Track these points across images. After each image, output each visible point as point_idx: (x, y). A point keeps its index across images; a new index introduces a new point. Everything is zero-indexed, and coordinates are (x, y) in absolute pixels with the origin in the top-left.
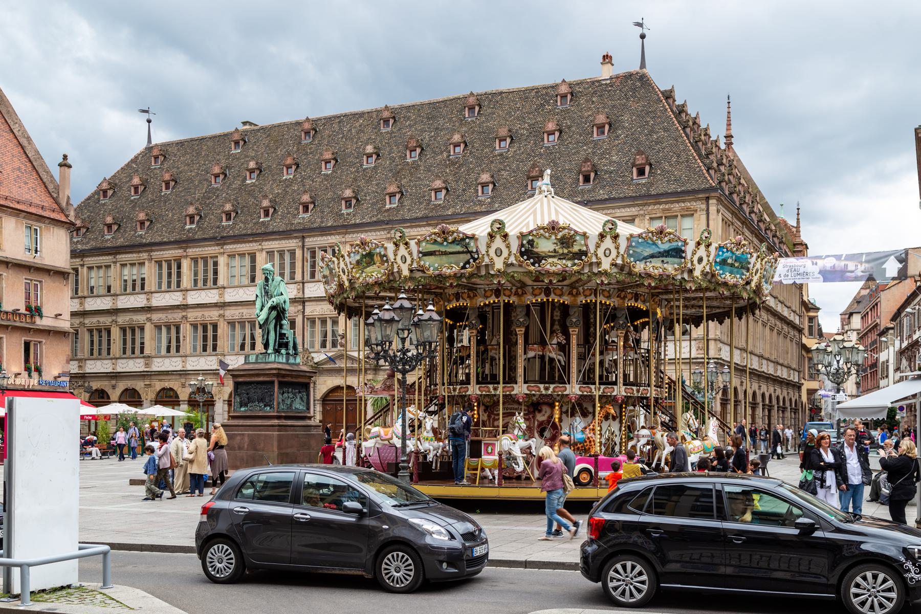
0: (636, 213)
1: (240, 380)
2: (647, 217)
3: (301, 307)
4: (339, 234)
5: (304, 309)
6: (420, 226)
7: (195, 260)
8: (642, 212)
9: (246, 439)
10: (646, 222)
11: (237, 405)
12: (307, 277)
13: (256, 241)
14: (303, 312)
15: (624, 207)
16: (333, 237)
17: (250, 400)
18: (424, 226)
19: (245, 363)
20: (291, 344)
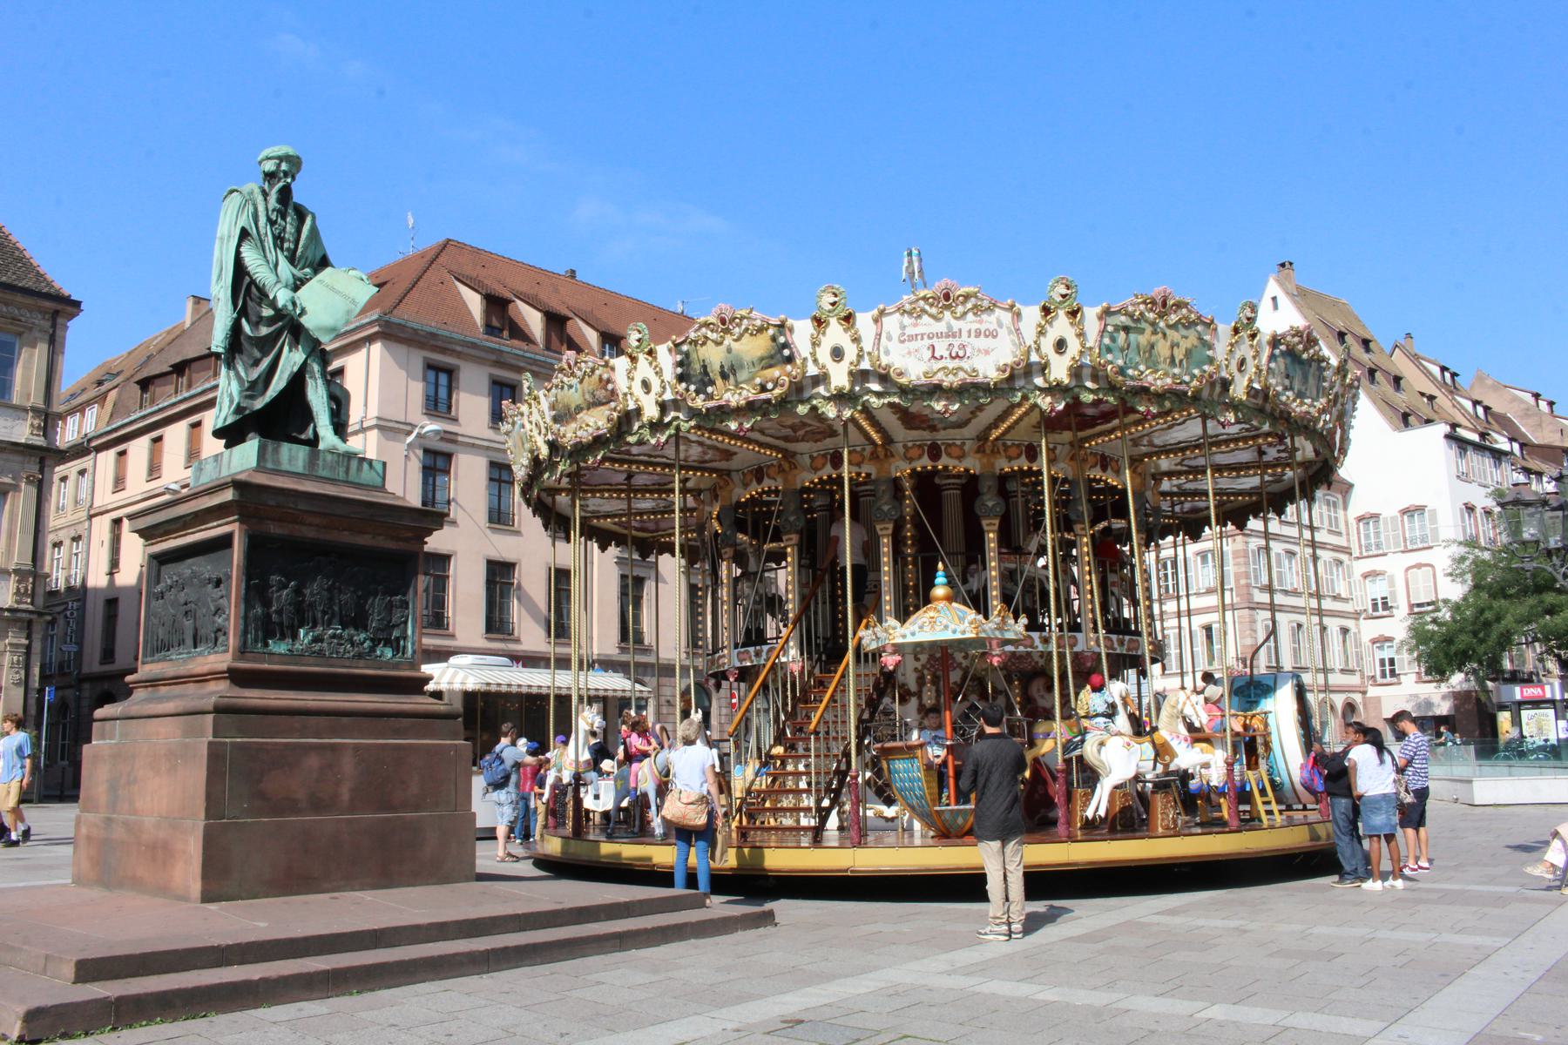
1: (274, 529)
9: (348, 765)
19: (261, 467)
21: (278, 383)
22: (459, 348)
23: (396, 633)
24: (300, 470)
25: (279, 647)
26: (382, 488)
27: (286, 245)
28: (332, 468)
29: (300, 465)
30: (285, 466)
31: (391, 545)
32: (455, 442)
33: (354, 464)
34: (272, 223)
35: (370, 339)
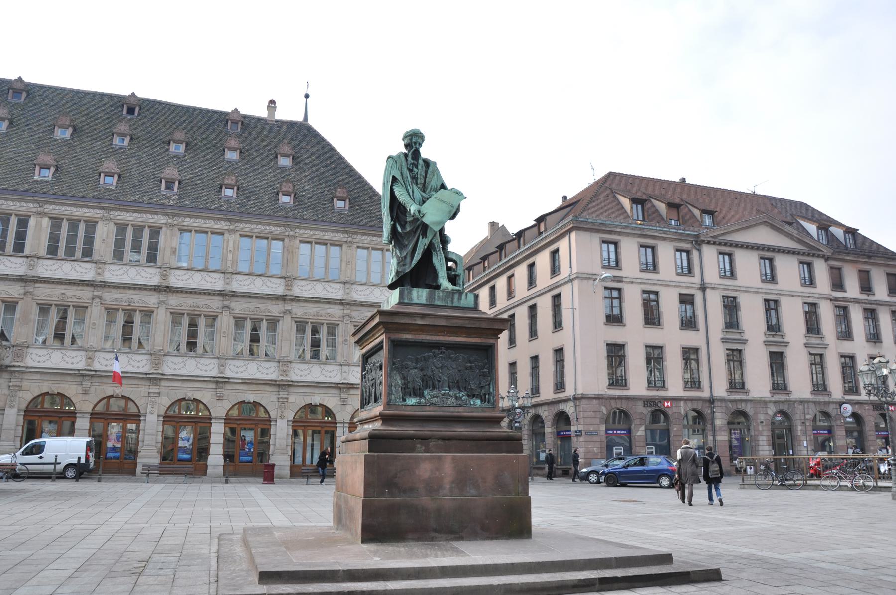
0: (345, 240)
6: (87, 207)
8: (350, 239)
11: (397, 393)
17: (430, 382)
18: (93, 208)
21: (417, 256)
22: (619, 230)
23: (483, 391)
24: (424, 302)
25: (411, 401)
26: (475, 309)
27: (419, 181)
29: (423, 300)
30: (415, 301)
32: (621, 281)
33: (456, 296)
34: (411, 171)
35: (569, 231)
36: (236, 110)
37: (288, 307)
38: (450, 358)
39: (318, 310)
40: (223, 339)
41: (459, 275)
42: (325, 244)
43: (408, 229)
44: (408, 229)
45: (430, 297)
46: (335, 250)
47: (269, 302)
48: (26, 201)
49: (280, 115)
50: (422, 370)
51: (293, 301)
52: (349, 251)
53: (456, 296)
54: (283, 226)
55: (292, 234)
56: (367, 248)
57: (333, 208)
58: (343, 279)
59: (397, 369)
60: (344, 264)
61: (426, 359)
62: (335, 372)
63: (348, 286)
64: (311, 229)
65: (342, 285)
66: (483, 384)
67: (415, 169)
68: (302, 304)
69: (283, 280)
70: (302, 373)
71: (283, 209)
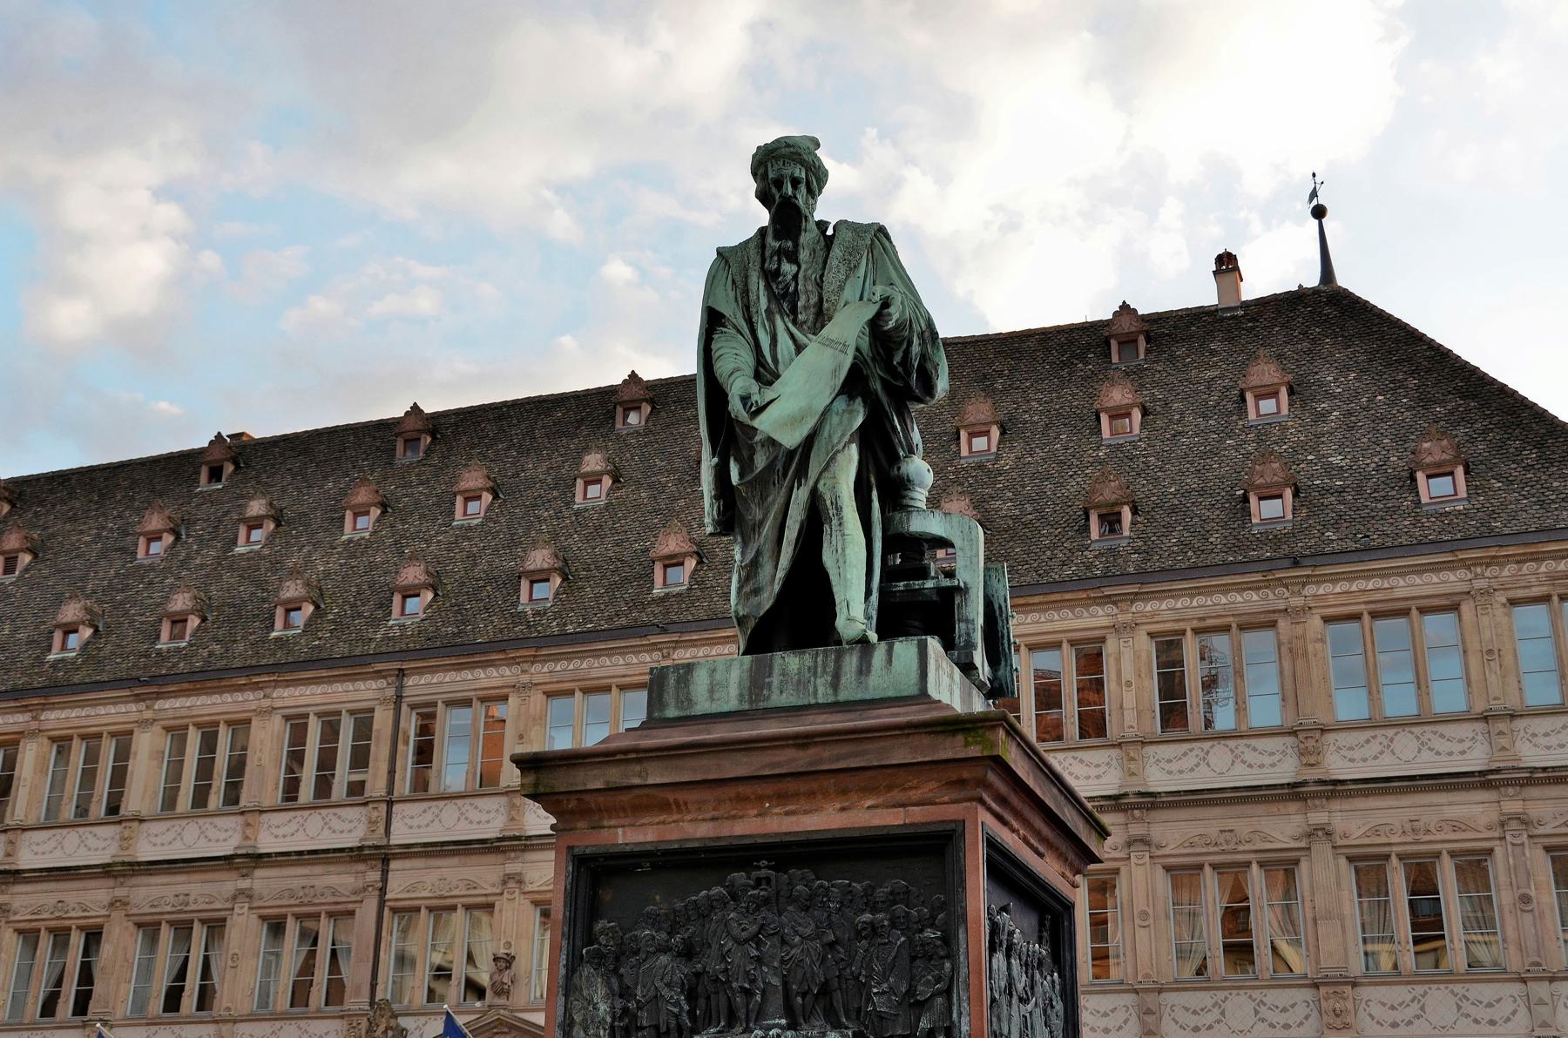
0: (1464, 587)
1: (628, 835)
2: (1501, 598)
3: (374, 876)
4: (512, 662)
5: (385, 880)
7: (62, 744)
8: (1480, 584)
10: (1499, 611)
12: (404, 786)
13: (256, 687)
14: (383, 891)
15: (1420, 570)
16: (493, 672)
20: (975, 611)
23: (924, 1024)
24: (732, 704)
26: (922, 696)
28: (801, 684)
30: (703, 705)
31: (891, 818)
33: (851, 662)
34: (771, 276)
36: (1125, 307)
37: (1318, 817)
38: (791, 899)
39: (1412, 813)
40: (1142, 934)
41: (963, 591)
42: (1405, 613)
43: (760, 461)
44: (760, 461)
45: (757, 683)
46: (1437, 627)
47: (1260, 809)
48: (636, 650)
49: (1256, 284)
50: (688, 953)
51: (1331, 796)
52: (1485, 620)
53: (851, 662)
54: (1267, 584)
55: (1297, 601)
56: (1545, 599)
57: (1418, 503)
58: (1480, 707)
59: (598, 959)
60: (1474, 663)
61: (703, 913)
62: (1506, 1007)
63: (1501, 726)
64: (1352, 577)
65: (1480, 726)
66: (923, 992)
67: (788, 268)
68: (1360, 803)
69: (1290, 740)
70: (1397, 1016)
71: (1273, 537)
